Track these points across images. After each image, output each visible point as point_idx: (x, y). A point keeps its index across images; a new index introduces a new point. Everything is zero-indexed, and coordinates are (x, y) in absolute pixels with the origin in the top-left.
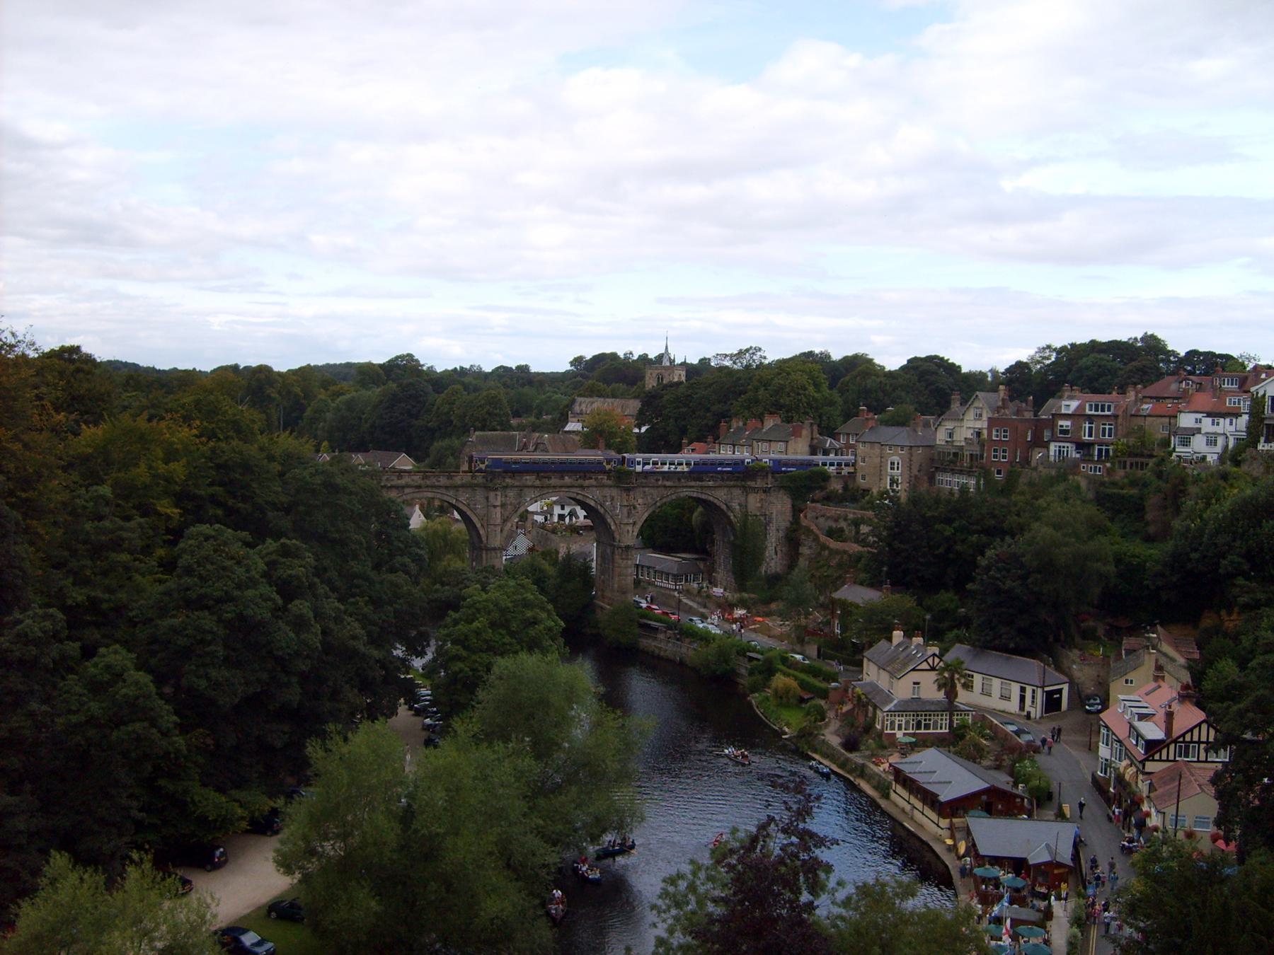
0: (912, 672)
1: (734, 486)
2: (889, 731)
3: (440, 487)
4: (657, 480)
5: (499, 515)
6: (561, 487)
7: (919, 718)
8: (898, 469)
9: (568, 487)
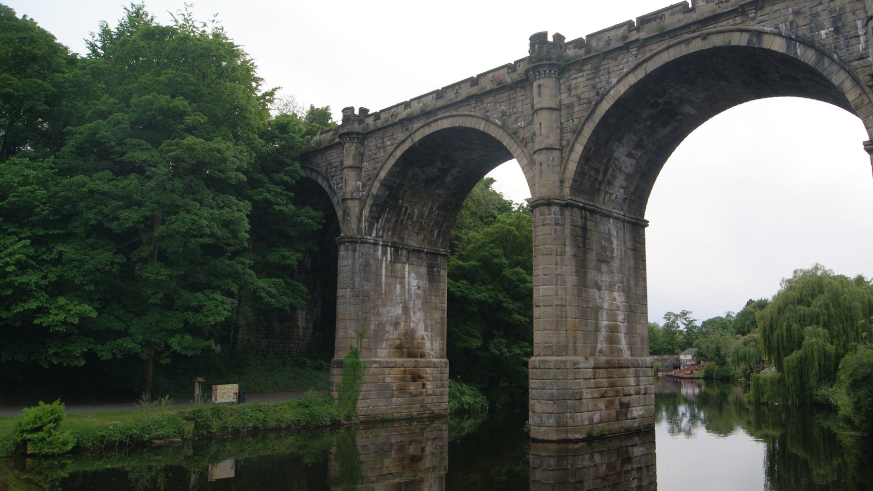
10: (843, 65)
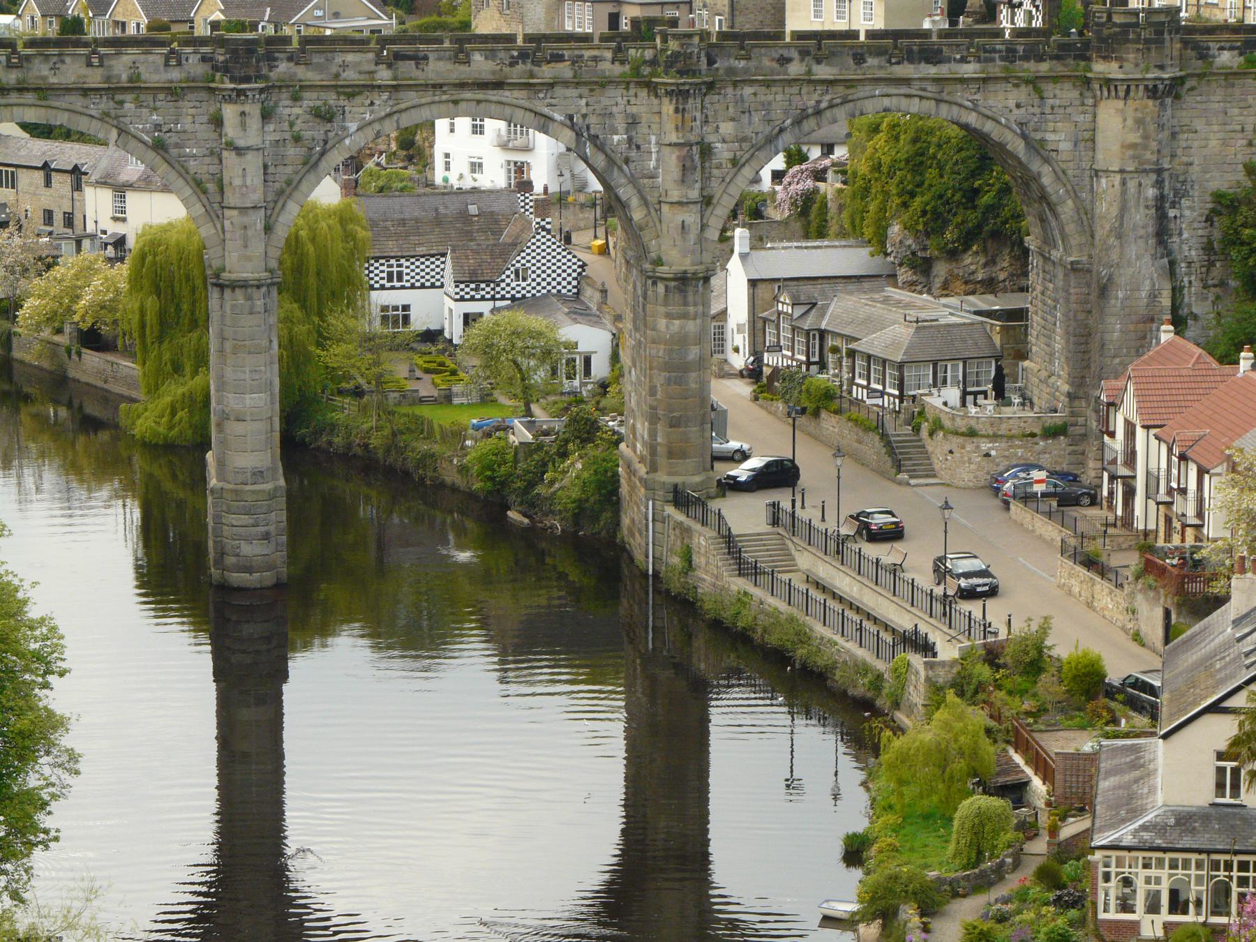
1: (1055, 79)
2: (1113, 915)
3: (68, 90)
4: (783, 61)
5: (255, 178)
6: (462, 85)
7: (1222, 873)
9: (483, 85)
10: (633, 181)
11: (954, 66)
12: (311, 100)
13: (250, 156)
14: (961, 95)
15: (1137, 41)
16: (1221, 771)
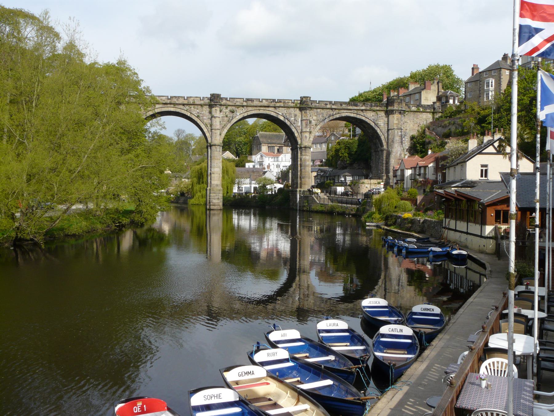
0: (478, 156)
3: (180, 104)
4: (326, 104)
5: (218, 123)
6: (261, 106)
8: (492, 86)
11: (360, 107)
12: (230, 108)
13: (217, 118)
14: (361, 113)
15: (397, 102)
16: (482, 171)
